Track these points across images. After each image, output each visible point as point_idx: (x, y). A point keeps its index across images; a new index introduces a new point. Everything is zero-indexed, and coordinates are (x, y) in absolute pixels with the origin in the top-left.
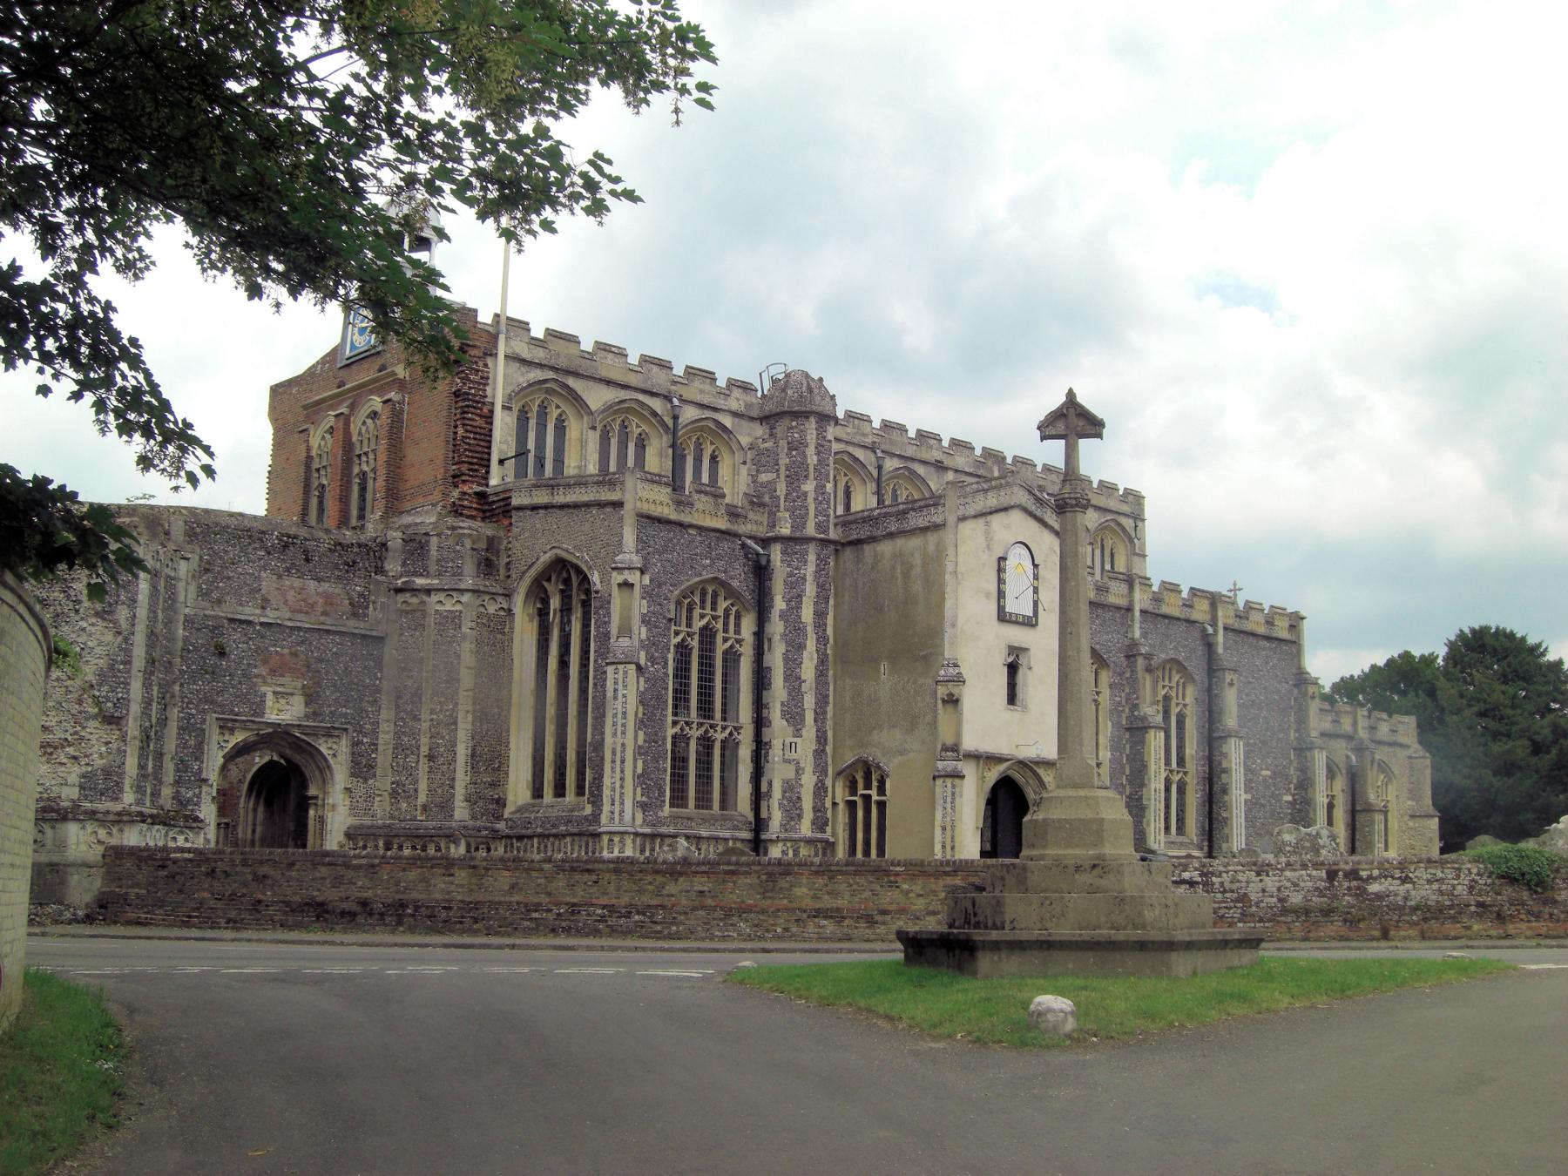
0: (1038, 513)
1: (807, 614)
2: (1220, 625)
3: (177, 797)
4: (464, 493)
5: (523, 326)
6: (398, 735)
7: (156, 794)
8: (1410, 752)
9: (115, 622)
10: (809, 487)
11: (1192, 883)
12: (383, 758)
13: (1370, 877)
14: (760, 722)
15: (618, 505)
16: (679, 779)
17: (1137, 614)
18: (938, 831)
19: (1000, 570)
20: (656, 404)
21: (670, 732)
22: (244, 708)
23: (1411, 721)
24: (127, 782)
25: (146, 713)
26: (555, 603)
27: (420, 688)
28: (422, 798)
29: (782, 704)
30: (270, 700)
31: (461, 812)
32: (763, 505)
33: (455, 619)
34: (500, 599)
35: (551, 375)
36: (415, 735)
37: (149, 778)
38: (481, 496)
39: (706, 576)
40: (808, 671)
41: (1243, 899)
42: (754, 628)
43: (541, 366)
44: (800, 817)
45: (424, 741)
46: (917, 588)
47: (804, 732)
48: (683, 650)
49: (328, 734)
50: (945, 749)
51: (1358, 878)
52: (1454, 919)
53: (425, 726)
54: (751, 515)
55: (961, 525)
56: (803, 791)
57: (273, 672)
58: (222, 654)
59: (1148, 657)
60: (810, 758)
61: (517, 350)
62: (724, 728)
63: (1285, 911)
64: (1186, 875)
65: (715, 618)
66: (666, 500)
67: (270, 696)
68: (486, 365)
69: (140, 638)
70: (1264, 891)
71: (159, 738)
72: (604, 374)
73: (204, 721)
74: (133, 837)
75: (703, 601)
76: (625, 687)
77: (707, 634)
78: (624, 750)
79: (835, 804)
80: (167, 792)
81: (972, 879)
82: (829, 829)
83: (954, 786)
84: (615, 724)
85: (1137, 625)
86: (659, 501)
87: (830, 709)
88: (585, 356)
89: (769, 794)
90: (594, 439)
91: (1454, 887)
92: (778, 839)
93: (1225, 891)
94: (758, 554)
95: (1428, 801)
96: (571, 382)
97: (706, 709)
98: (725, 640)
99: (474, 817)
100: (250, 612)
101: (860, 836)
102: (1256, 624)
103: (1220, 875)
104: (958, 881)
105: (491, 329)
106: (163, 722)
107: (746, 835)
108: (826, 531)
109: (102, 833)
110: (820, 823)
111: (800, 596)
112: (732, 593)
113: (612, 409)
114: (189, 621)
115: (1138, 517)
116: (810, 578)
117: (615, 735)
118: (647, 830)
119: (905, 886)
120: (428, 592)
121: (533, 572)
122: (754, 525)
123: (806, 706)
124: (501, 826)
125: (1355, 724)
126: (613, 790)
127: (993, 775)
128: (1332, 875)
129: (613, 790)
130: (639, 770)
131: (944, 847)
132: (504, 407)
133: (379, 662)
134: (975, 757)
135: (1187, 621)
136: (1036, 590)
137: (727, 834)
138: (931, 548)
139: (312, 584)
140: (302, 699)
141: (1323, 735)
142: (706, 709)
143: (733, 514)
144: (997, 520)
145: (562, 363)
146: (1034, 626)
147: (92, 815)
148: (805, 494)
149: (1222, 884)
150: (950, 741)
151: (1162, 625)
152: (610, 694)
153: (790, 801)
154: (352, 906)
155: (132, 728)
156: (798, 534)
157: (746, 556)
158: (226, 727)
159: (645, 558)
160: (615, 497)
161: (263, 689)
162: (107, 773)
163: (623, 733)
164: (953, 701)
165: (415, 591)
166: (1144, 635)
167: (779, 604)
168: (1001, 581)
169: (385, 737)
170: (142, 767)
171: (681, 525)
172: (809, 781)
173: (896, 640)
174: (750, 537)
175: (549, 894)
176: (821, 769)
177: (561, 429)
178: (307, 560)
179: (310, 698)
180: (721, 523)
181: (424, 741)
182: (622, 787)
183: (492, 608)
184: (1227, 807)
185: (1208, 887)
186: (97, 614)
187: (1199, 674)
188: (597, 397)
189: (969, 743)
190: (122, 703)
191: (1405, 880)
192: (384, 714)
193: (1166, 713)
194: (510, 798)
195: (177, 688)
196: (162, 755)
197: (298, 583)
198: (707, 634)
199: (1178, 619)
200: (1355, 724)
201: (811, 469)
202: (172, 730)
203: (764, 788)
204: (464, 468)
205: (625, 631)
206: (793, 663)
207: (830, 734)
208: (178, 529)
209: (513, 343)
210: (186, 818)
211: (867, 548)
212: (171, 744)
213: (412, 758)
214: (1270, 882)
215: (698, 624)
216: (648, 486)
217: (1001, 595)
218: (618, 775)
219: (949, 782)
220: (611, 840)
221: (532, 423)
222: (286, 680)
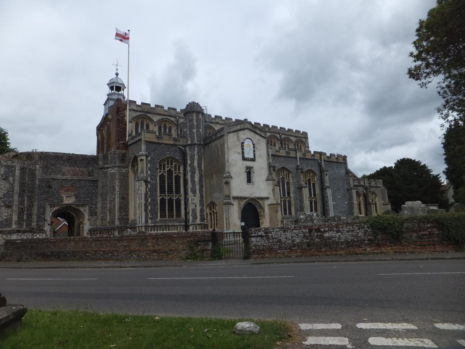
0: (254, 130)
1: (196, 164)
3: (37, 225)
4: (120, 144)
5: (135, 102)
6: (102, 204)
8: (381, 189)
9: (9, 181)
10: (195, 131)
11: (262, 236)
12: (99, 210)
13: (325, 231)
14: (186, 193)
15: (141, 140)
17: (298, 159)
18: (225, 220)
19: (242, 146)
20: (173, 119)
22: (57, 201)
23: (381, 181)
24: (13, 223)
27: (107, 192)
28: (108, 220)
29: (191, 188)
30: (64, 199)
31: (117, 223)
32: (185, 137)
33: (113, 175)
34: (126, 168)
35: (143, 113)
38: (124, 143)
39: (168, 156)
40: (197, 179)
41: (280, 241)
42: (183, 169)
43: (140, 111)
44: (197, 218)
45: (108, 205)
46: (220, 153)
47: (196, 195)
48: (162, 177)
49: (83, 206)
50: (226, 196)
51: (320, 231)
52: (359, 246)
53: (108, 201)
54: (181, 140)
55: (229, 135)
56: (197, 211)
57: (66, 191)
58: (50, 187)
59: (302, 169)
60: (198, 202)
61: (133, 108)
62: (176, 196)
63: (294, 246)
64: (260, 233)
65: (172, 167)
66: (154, 137)
67: (65, 197)
68: (124, 112)
70: (286, 238)
72: (158, 112)
73: (45, 205)
74: (14, 237)
75: (168, 164)
76: (141, 187)
77: (170, 172)
78: (141, 204)
79: (207, 214)
81: (195, 238)
82: (205, 221)
83: (228, 207)
84: (139, 197)
85: (298, 162)
86: (152, 138)
87: (204, 189)
88: (152, 108)
89: (189, 213)
91: (358, 233)
92: (191, 225)
94: (182, 149)
95: (387, 200)
96: (149, 115)
97: (170, 191)
98: (175, 173)
99: (121, 224)
100: (59, 177)
101: (213, 222)
102: (333, 159)
103: (271, 233)
104: (191, 239)
105: (125, 103)
106: (31, 206)
107: (183, 224)
108: (200, 142)
109: (4, 237)
110: (202, 219)
111: (194, 160)
112: (176, 161)
113: (160, 121)
115: (306, 138)
117: (139, 200)
118: (153, 225)
119: (177, 241)
120: (108, 168)
121: (131, 160)
122: (181, 142)
123: (197, 188)
124: (128, 225)
125: (364, 183)
126: (139, 215)
127: (243, 203)
128: (310, 231)
129: (139, 215)
131: (227, 224)
132: (129, 122)
133: (97, 187)
134: (234, 198)
135: (313, 159)
137: (178, 224)
138: (222, 142)
139: (78, 169)
140: (74, 197)
141: (354, 186)
142: (170, 191)
143: (175, 140)
144: (241, 133)
145: (146, 110)
148: (194, 133)
149: (272, 236)
150: (228, 194)
153: (194, 214)
154: (49, 253)
155: (15, 208)
156: (192, 143)
157: (180, 150)
160: (140, 138)
161: (63, 195)
162: (7, 220)
163: (141, 199)
164: (227, 183)
165: (105, 168)
167: (189, 162)
169: (99, 205)
172: (198, 208)
173: (217, 169)
174: (181, 145)
175: (91, 248)
176: (202, 204)
178: (75, 163)
179: (77, 197)
181: (108, 205)
182: (141, 214)
183: (124, 171)
184: (328, 206)
185: (267, 237)
186: (3, 179)
187: (318, 173)
188: (156, 118)
191: (338, 231)
192: (99, 200)
193: (310, 184)
194: (130, 218)
195: (37, 197)
196: (31, 215)
197: (73, 169)
198: (170, 172)
199: (311, 159)
200: (364, 183)
201: (195, 126)
203: (188, 211)
204: (120, 137)
205: (142, 172)
206: (193, 177)
207: (204, 195)
209: (132, 106)
210: (40, 230)
211: (210, 145)
213: (106, 210)
214: (288, 235)
215: (167, 169)
216: (148, 134)
217: (243, 153)
218: (140, 211)
220: (139, 228)
221: (140, 126)
222: (70, 193)
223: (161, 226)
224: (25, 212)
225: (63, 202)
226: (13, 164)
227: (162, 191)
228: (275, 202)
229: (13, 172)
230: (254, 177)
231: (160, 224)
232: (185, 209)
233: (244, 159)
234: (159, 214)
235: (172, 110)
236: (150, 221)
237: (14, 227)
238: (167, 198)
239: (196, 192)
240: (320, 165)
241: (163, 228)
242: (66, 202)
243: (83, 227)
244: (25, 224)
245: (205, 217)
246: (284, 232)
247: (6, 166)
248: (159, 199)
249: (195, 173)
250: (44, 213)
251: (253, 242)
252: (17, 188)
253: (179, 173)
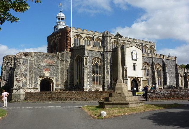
2: (165, 59)
3: (34, 86)
7: (32, 86)
10: (108, 45)
11: (152, 93)
16: (94, 81)
19: (132, 54)
21: (92, 75)
24: (28, 84)
25: (30, 76)
26: (78, 61)
30: (45, 74)
31: (69, 86)
36: (63, 77)
40: (109, 67)
41: (159, 95)
48: (93, 66)
49: (53, 77)
58: (39, 68)
64: (151, 92)
69: (28, 68)
71: (32, 79)
72: (85, 33)
74: (29, 91)
79: (113, 83)
80: (33, 85)
90: (84, 41)
96: (80, 34)
100: (42, 64)
106: (32, 77)
109: (25, 90)
112: (99, 59)
114: (35, 65)
120: (64, 60)
130: (88, 80)
134: (129, 77)
136: (137, 56)
147: (23, 88)
151: (157, 59)
152: (84, 71)
155: (28, 78)
158: (40, 77)
162: (25, 83)
166: (154, 61)
167: (105, 60)
168: (132, 55)
170: (30, 82)
171: (93, 51)
172: (109, 81)
177: (80, 40)
179: (50, 73)
180: (97, 50)
185: (154, 93)
190: (27, 75)
193: (158, 70)
194: (75, 84)
202: (33, 78)
208: (33, 54)
212: (33, 80)
217: (132, 57)
219: (126, 80)
226: (27, 58)
227: (93, 73)
228: (145, 79)
229: (27, 62)
230: (137, 68)
231: (93, 87)
237: (28, 86)
240: (163, 61)
247: (25, 59)
249: (108, 65)
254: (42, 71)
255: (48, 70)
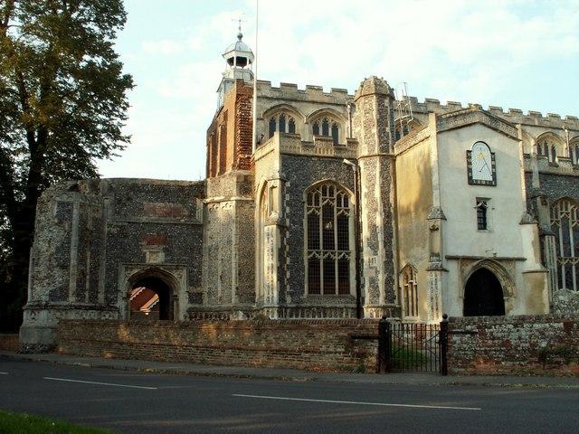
3: (106, 298)
5: (268, 83)
11: (473, 333)
19: (469, 158)
24: (71, 293)
30: (148, 256)
35: (283, 102)
37: (79, 294)
41: (506, 343)
43: (277, 99)
44: (378, 296)
48: (313, 219)
49: (177, 268)
57: (149, 243)
64: (469, 328)
65: (332, 200)
70: (520, 338)
74: (72, 316)
75: (324, 194)
80: (101, 297)
82: (396, 301)
89: (363, 286)
93: (494, 339)
96: (293, 104)
98: (339, 210)
106: (96, 267)
109: (58, 314)
114: (110, 225)
116: (378, 175)
127: (469, 269)
134: (449, 258)
137: (342, 305)
145: (288, 96)
146: (495, 185)
147: (53, 307)
149: (492, 333)
159: (287, 174)
162: (61, 289)
167: (364, 190)
168: (469, 163)
172: (381, 278)
180: (331, 153)
185: (483, 334)
189: (453, 251)
194: (257, 292)
217: (470, 170)
221: (278, 125)
223: (310, 308)
224: (88, 277)
225: (145, 261)
227: (314, 244)
229: (70, 212)
232: (358, 279)
233: (471, 182)
234: (306, 286)
235: (338, 94)
236: (289, 299)
238: (321, 258)
239: (378, 247)
241: (314, 312)
242: (152, 262)
243: (178, 305)
244: (87, 296)
245: (396, 294)
246: (515, 326)
247: (60, 204)
248: (306, 258)
250: (116, 279)
251: (455, 343)
252: (74, 238)
253: (346, 210)
254: (137, 246)
255: (159, 243)
